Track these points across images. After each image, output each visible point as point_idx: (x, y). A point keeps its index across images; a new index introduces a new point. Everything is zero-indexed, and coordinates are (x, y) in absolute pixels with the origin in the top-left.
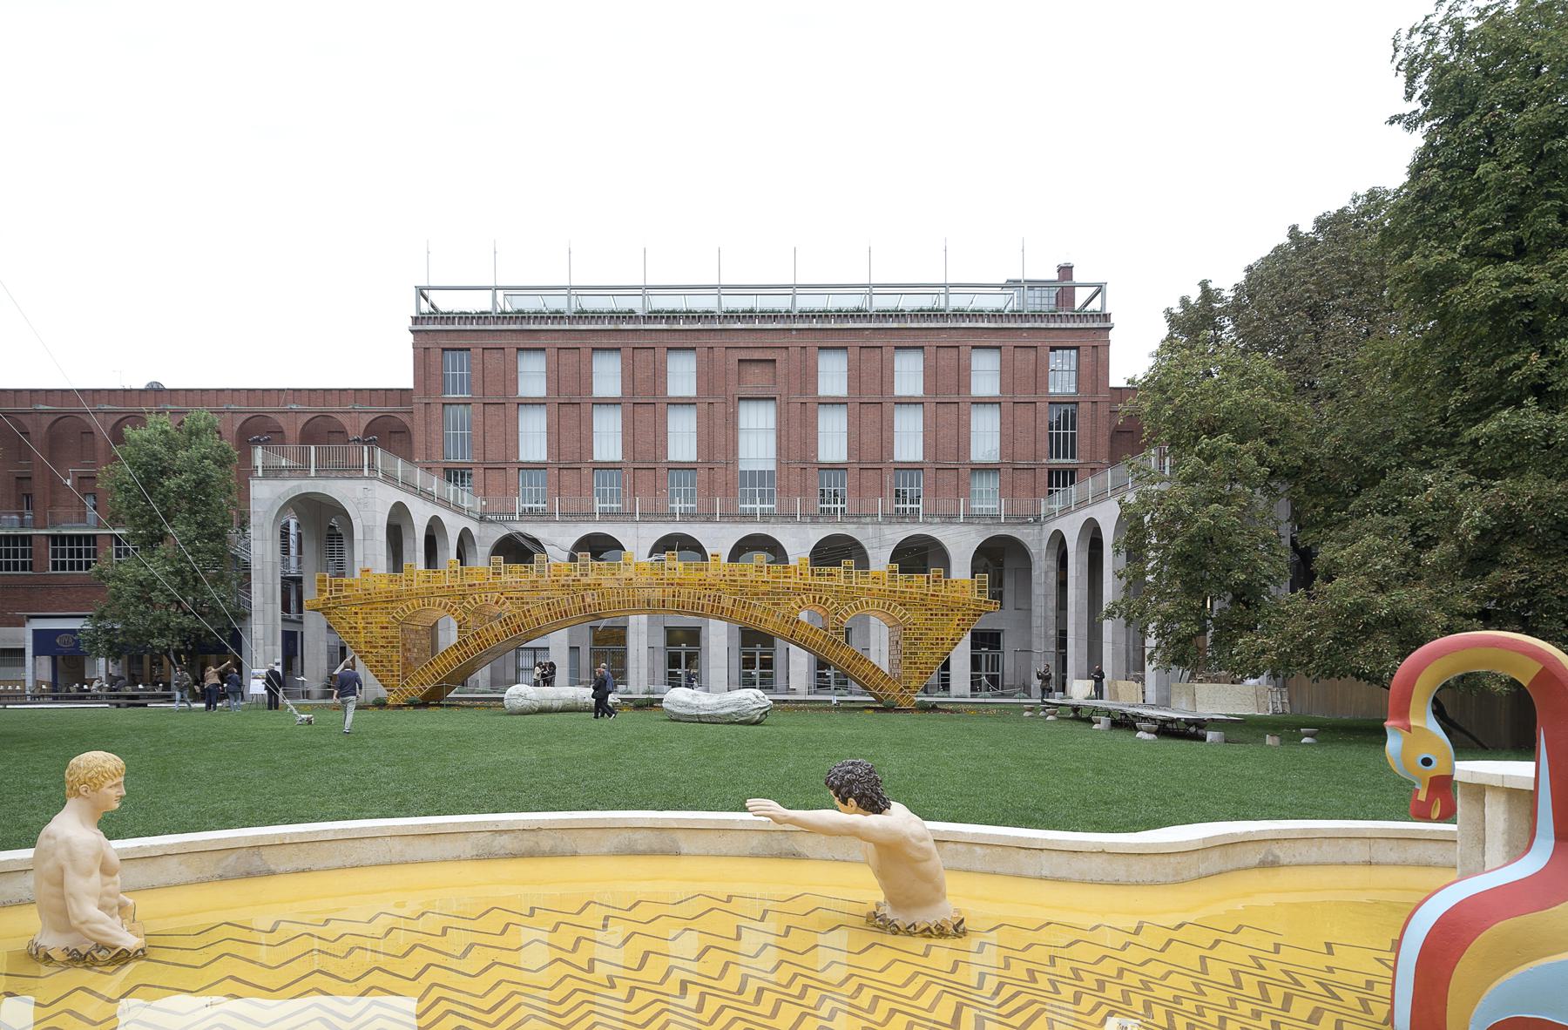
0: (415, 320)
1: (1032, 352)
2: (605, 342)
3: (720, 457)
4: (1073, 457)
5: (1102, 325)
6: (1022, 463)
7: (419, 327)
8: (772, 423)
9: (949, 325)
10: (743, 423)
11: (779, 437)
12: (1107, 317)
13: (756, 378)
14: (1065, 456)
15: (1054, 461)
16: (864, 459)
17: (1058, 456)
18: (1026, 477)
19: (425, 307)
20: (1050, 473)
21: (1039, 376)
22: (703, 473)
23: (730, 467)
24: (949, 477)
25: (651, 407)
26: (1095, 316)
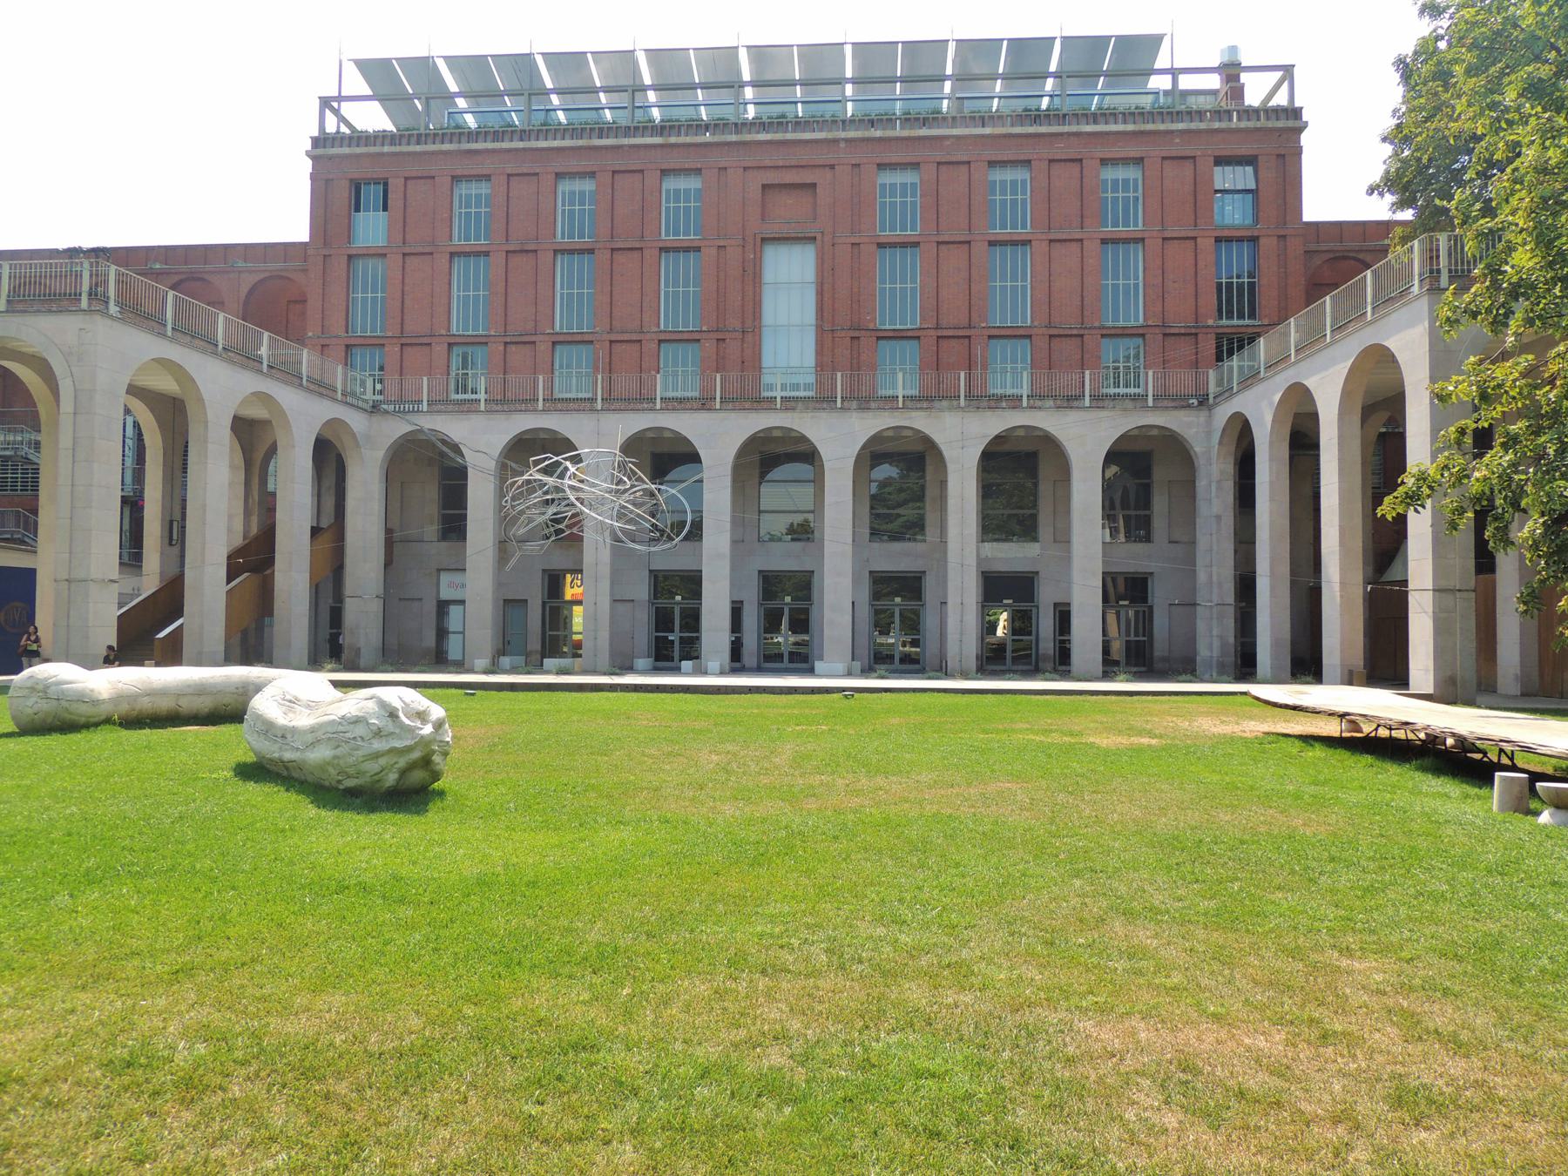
0: (316, 142)
1: (1189, 165)
2: (574, 164)
3: (734, 323)
4: (1252, 315)
5: (1290, 123)
6: (1178, 326)
7: (320, 151)
8: (810, 274)
9: (1066, 129)
10: (769, 275)
11: (820, 293)
12: (1294, 113)
13: (788, 208)
14: (1241, 316)
15: (1224, 322)
16: (944, 323)
17: (1230, 317)
18: (1184, 349)
19: (331, 125)
20: (1219, 337)
21: (1201, 196)
22: (710, 346)
23: (749, 337)
24: (1069, 346)
25: (636, 255)
26: (1278, 112)
